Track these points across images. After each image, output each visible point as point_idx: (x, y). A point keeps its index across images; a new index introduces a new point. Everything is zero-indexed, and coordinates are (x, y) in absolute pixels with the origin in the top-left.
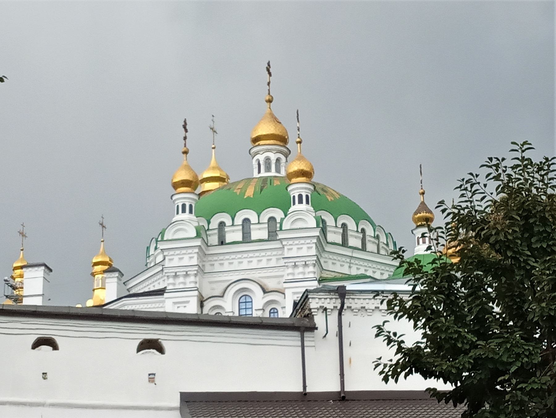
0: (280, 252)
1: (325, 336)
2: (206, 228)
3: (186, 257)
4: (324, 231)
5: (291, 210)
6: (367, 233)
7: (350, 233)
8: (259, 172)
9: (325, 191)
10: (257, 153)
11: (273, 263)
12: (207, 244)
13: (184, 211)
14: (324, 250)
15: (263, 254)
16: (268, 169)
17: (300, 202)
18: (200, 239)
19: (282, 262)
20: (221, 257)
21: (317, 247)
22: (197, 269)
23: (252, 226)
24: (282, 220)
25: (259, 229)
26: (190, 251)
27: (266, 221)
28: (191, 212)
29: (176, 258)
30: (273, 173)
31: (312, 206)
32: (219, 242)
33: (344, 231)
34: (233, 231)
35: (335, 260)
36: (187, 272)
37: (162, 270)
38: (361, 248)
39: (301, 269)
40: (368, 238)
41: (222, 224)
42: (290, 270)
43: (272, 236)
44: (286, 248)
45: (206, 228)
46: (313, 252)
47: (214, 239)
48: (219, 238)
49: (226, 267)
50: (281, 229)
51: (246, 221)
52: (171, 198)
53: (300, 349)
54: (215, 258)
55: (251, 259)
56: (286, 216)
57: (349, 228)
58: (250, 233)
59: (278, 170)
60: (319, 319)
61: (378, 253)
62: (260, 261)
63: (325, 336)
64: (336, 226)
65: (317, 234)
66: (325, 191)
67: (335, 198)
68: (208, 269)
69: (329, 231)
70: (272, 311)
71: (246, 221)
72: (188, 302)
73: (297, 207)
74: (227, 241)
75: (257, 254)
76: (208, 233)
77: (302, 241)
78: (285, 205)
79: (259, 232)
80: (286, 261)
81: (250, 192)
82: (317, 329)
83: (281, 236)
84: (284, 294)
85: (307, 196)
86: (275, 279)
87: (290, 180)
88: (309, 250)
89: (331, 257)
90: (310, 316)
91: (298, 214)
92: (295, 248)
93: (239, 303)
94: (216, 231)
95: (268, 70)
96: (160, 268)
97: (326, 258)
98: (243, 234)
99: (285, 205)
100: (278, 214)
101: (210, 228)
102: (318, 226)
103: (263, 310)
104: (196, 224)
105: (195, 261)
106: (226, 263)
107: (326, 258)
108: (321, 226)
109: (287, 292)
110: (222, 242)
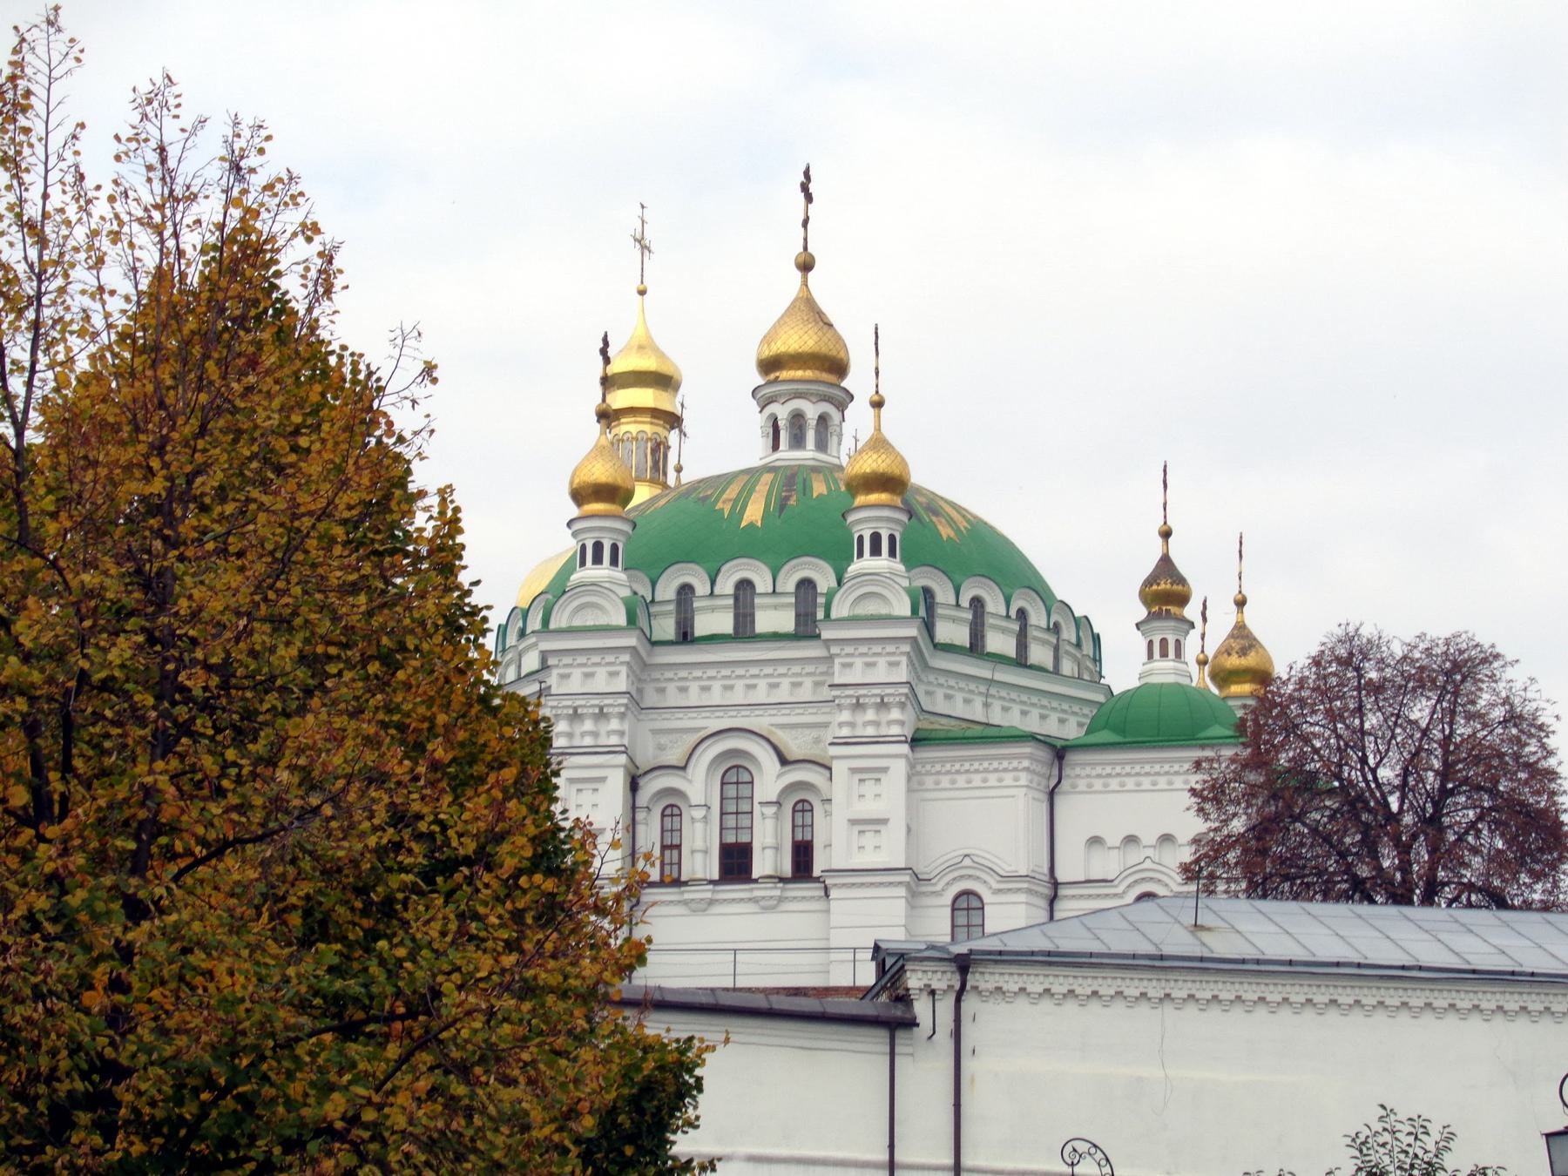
0: (822, 668)
2: (649, 599)
3: (601, 673)
7: (990, 621)
9: (936, 513)
11: (806, 693)
13: (598, 559)
14: (926, 666)
15: (782, 670)
17: (876, 551)
19: (827, 693)
20: (683, 674)
21: (911, 663)
22: (625, 701)
23: (757, 601)
25: (776, 607)
28: (614, 562)
29: (577, 673)
30: (808, 454)
31: (904, 561)
32: (677, 633)
33: (975, 616)
35: (952, 687)
36: (601, 709)
39: (870, 715)
41: (686, 591)
42: (845, 716)
43: (806, 629)
44: (837, 661)
46: (902, 674)
47: (666, 627)
48: (678, 623)
49: (694, 698)
50: (827, 615)
54: (669, 674)
56: (839, 583)
58: (753, 615)
62: (775, 686)
68: (651, 699)
71: (745, 586)
72: (603, 780)
73: (867, 563)
74: (698, 632)
76: (653, 609)
77: (877, 649)
78: (840, 553)
79: (774, 617)
80: (836, 692)
81: (754, 512)
84: (830, 769)
85: (892, 538)
86: (807, 731)
87: (854, 496)
88: (891, 670)
89: (942, 680)
90: (904, 999)
91: (872, 583)
92: (859, 662)
93: (723, 784)
94: (672, 607)
97: (930, 683)
98: (736, 617)
101: (657, 599)
102: (915, 610)
103: (778, 803)
104: (626, 593)
105: (621, 684)
106: (694, 687)
108: (922, 612)
110: (685, 636)
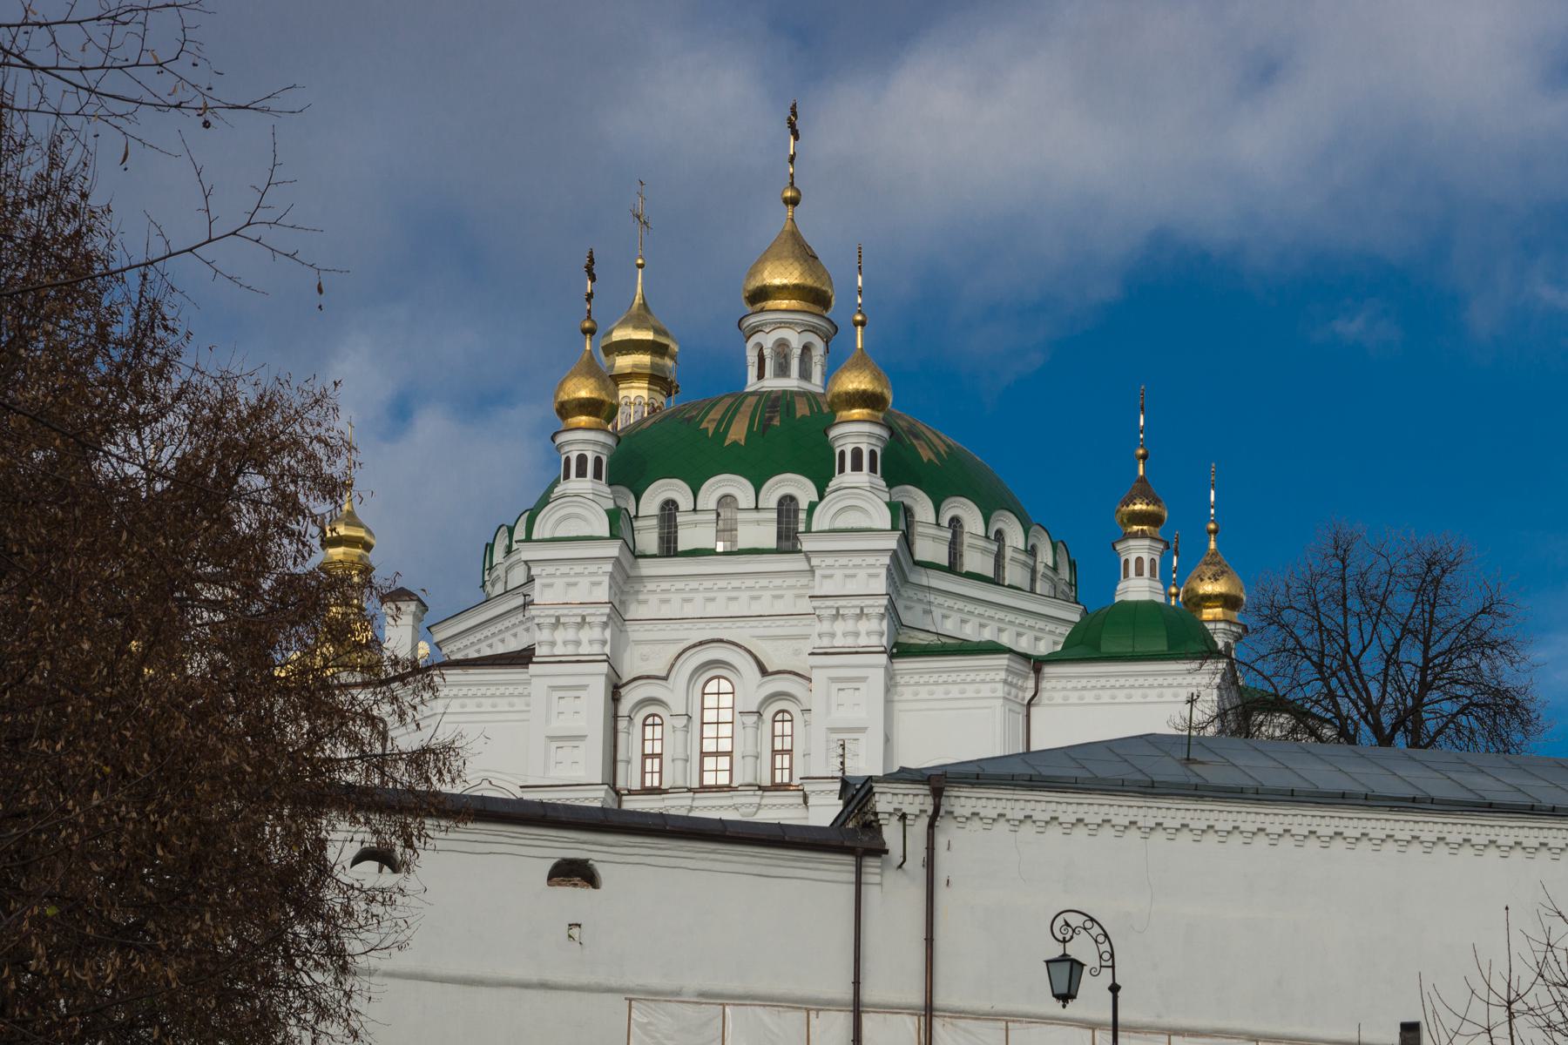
0: (804, 581)
1: (900, 866)
4: (907, 540)
5: (833, 484)
6: (1008, 542)
7: (967, 539)
8: (761, 376)
10: (756, 330)
12: (633, 553)
13: (581, 473)
14: (905, 581)
16: (783, 370)
17: (857, 467)
18: (619, 542)
20: (665, 585)
24: (812, 507)
25: (758, 522)
26: (593, 568)
27: (774, 504)
28: (597, 475)
30: (792, 383)
33: (954, 535)
34: (696, 524)
37: (525, 606)
38: (992, 575)
40: (1009, 553)
41: (670, 507)
42: (826, 626)
43: (788, 541)
45: (633, 513)
47: (649, 539)
50: (808, 530)
51: (726, 501)
52: (553, 439)
53: (853, 887)
55: (734, 594)
57: (966, 529)
59: (805, 374)
60: (891, 833)
61: (1032, 591)
63: (900, 866)
64: (938, 524)
65: (893, 545)
66: (917, 437)
67: (938, 454)
69: (923, 535)
70: (779, 717)
75: (750, 582)
78: (822, 469)
80: (817, 603)
81: (738, 432)
82: (886, 852)
83: (807, 544)
90: (872, 827)
94: (655, 522)
95: (792, 126)
96: (520, 601)
97: (909, 598)
99: (822, 469)
100: (801, 488)
104: (611, 505)
105: (602, 594)
107: (909, 598)
108: (902, 526)
109: (815, 675)
110: (669, 548)
